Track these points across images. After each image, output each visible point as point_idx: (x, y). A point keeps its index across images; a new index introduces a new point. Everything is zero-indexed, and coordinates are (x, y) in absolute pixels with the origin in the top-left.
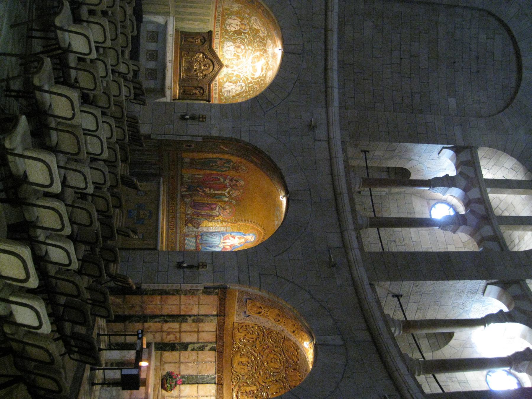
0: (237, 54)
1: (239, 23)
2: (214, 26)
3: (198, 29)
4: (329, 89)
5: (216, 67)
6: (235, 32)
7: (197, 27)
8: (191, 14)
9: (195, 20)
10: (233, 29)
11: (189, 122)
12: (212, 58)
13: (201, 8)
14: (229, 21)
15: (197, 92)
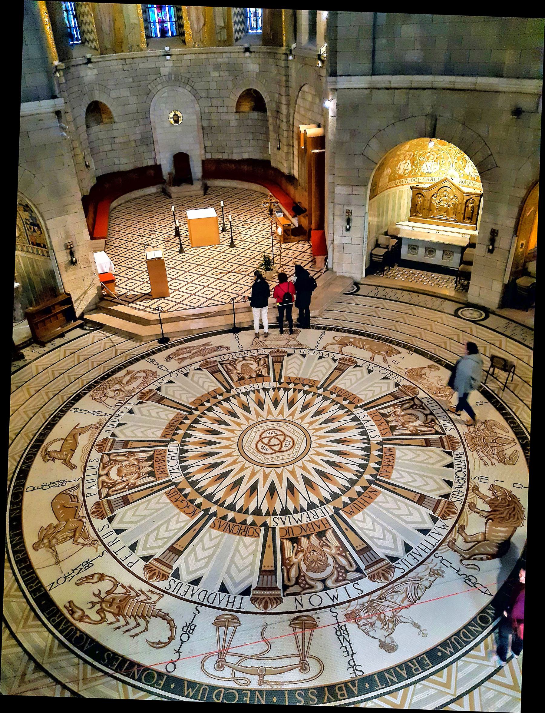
0: (435, 159)
1: (404, 162)
2: (406, 185)
3: (408, 199)
4: (478, 88)
5: (446, 184)
6: (413, 163)
7: (405, 213)
8: (393, 209)
9: (400, 204)
10: (410, 165)
11: (496, 245)
12: (437, 188)
13: (388, 202)
14: (401, 172)
15: (471, 205)
